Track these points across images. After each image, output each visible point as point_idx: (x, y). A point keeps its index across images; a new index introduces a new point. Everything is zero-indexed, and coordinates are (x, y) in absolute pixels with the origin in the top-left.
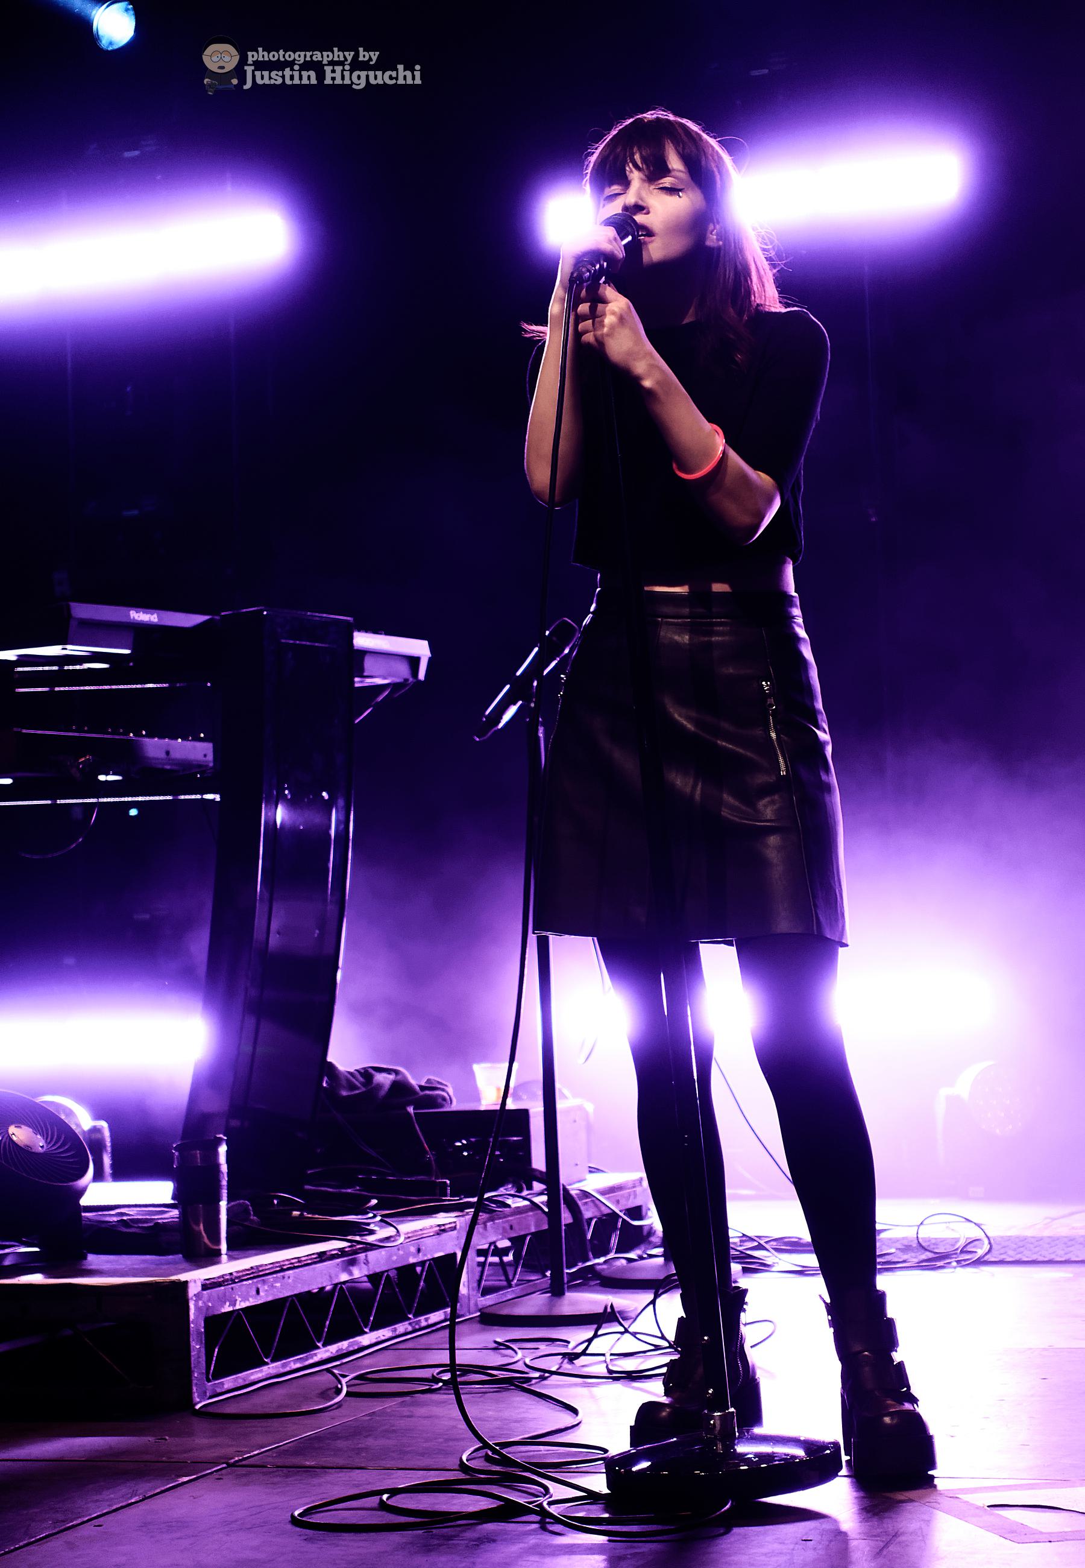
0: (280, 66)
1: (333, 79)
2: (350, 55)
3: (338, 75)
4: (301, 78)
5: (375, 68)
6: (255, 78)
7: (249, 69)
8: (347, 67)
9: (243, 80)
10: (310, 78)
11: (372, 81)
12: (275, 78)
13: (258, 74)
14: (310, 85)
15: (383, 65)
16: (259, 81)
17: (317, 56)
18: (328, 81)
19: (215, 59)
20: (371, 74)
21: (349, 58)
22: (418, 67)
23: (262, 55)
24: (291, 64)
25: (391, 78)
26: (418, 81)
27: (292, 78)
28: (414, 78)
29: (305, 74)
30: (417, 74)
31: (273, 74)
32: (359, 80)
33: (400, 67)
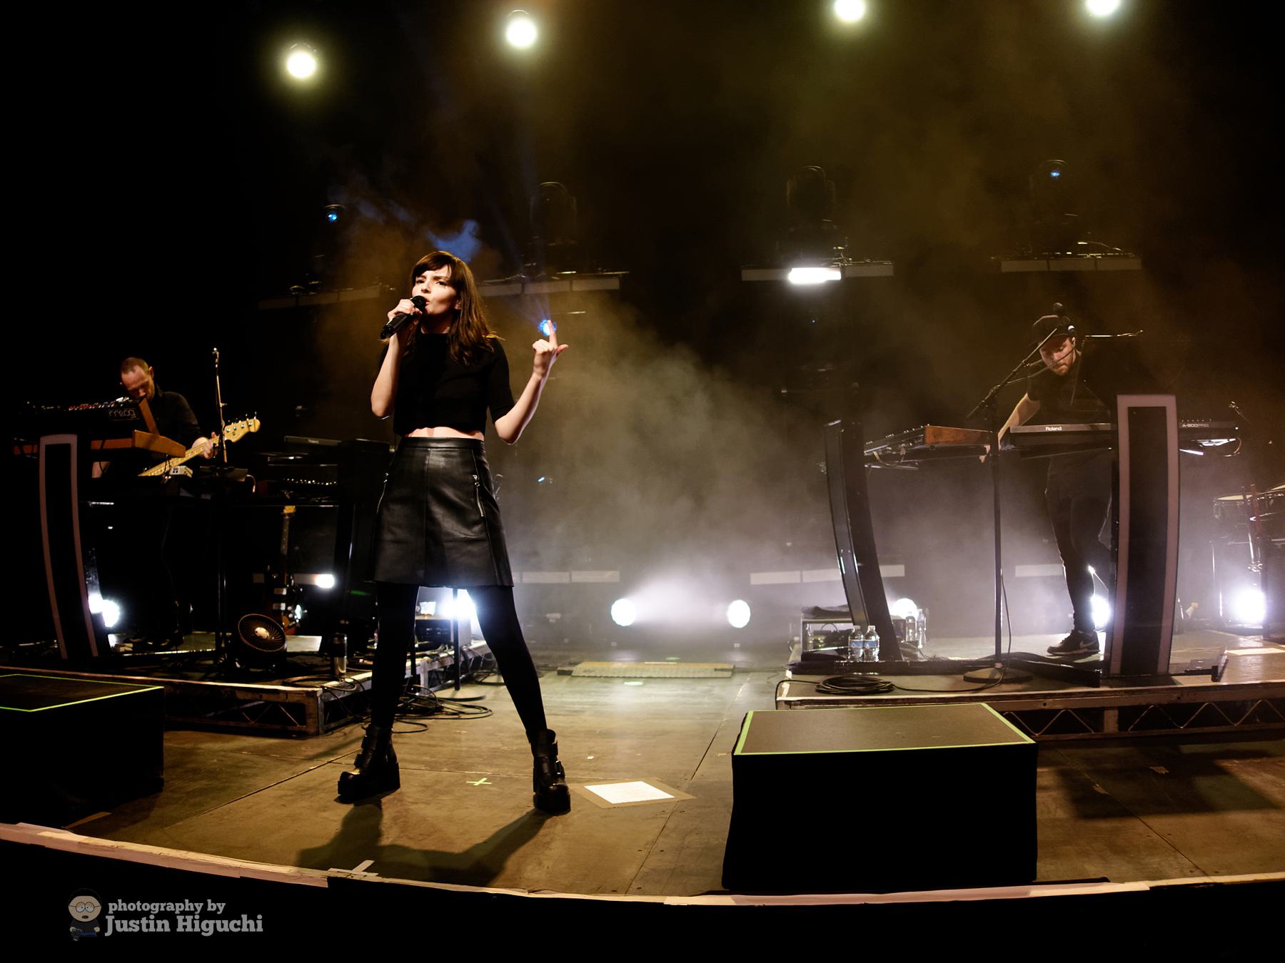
0: (137, 915)
1: (185, 927)
2: (199, 906)
3: (189, 924)
4: (156, 926)
5: (221, 917)
6: (116, 926)
7: (110, 919)
8: (197, 917)
9: (104, 929)
10: (164, 926)
11: (220, 929)
12: (133, 926)
13: (118, 922)
14: (164, 933)
15: (229, 915)
16: (119, 929)
17: (170, 907)
18: (180, 929)
19: (79, 909)
20: (219, 922)
21: (199, 909)
22: (260, 917)
23: (121, 906)
24: (147, 914)
25: (236, 926)
26: (260, 929)
27: (148, 926)
28: (256, 926)
29: (160, 923)
30: (260, 923)
31: (131, 922)
32: (207, 928)
33: (244, 917)
